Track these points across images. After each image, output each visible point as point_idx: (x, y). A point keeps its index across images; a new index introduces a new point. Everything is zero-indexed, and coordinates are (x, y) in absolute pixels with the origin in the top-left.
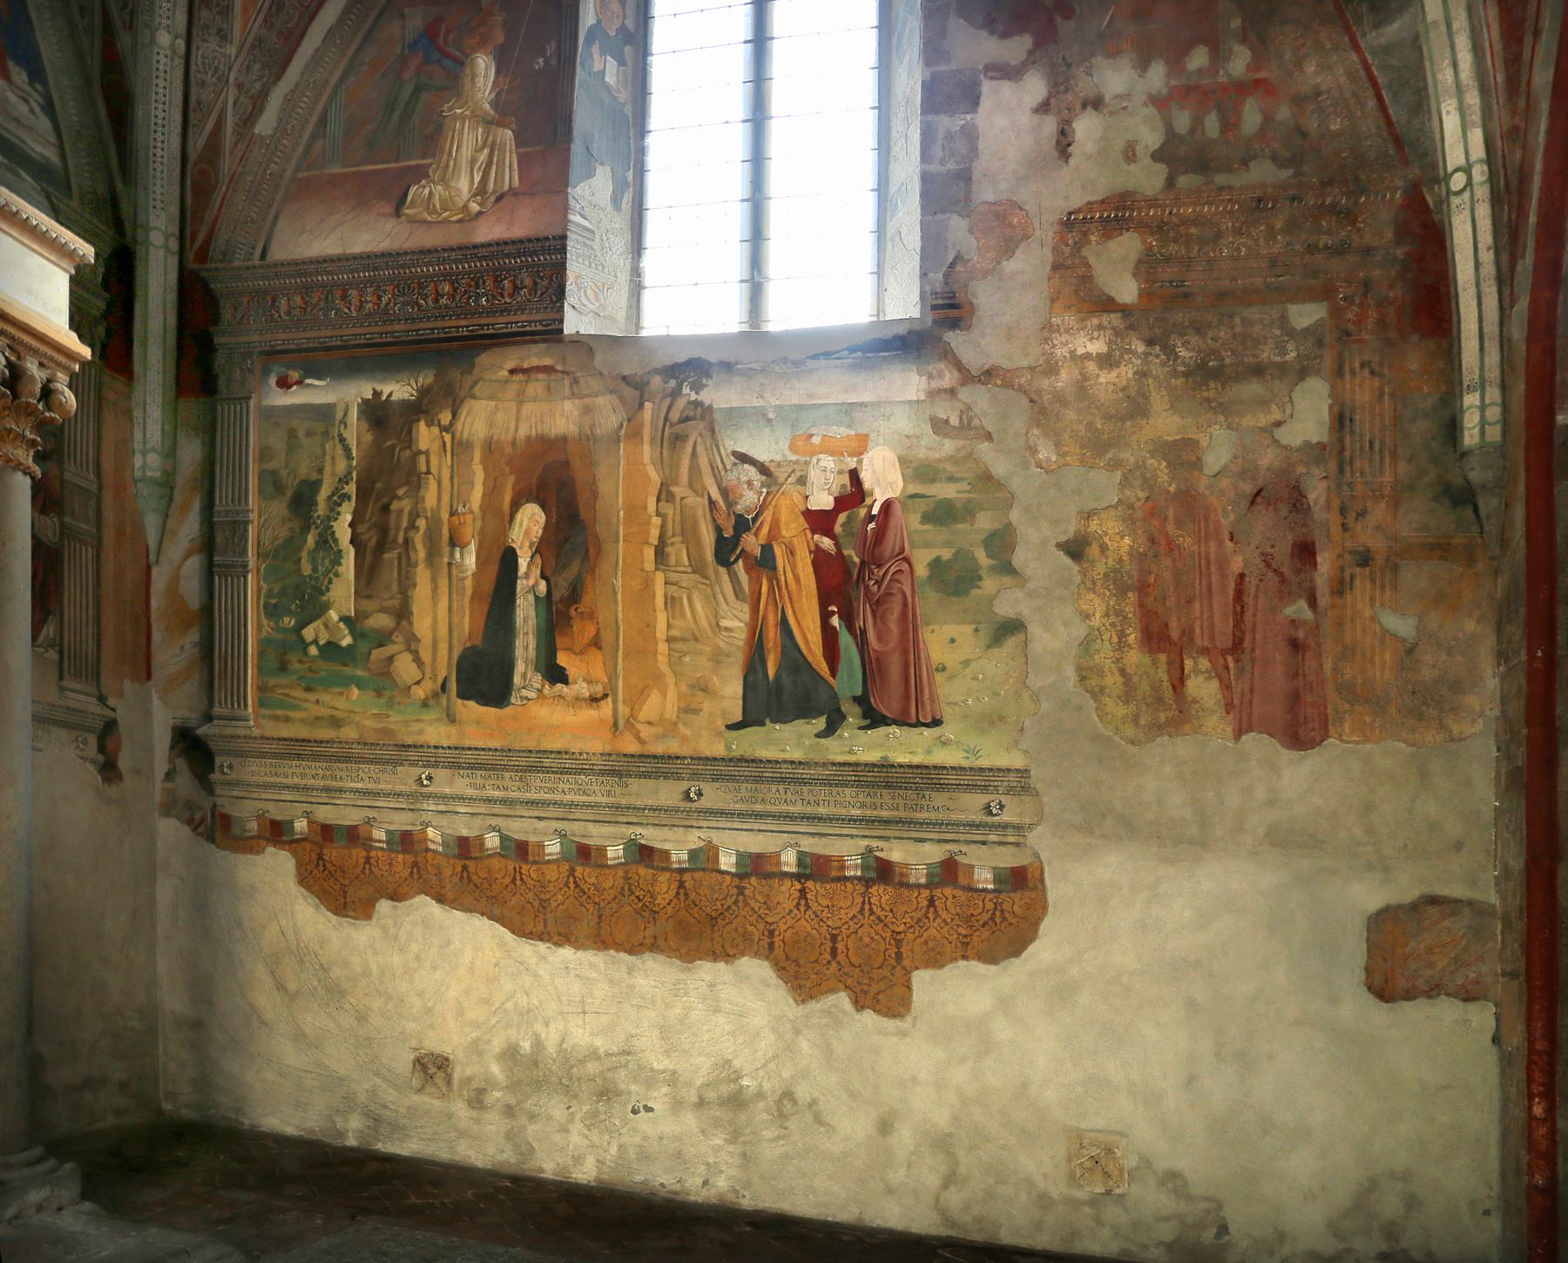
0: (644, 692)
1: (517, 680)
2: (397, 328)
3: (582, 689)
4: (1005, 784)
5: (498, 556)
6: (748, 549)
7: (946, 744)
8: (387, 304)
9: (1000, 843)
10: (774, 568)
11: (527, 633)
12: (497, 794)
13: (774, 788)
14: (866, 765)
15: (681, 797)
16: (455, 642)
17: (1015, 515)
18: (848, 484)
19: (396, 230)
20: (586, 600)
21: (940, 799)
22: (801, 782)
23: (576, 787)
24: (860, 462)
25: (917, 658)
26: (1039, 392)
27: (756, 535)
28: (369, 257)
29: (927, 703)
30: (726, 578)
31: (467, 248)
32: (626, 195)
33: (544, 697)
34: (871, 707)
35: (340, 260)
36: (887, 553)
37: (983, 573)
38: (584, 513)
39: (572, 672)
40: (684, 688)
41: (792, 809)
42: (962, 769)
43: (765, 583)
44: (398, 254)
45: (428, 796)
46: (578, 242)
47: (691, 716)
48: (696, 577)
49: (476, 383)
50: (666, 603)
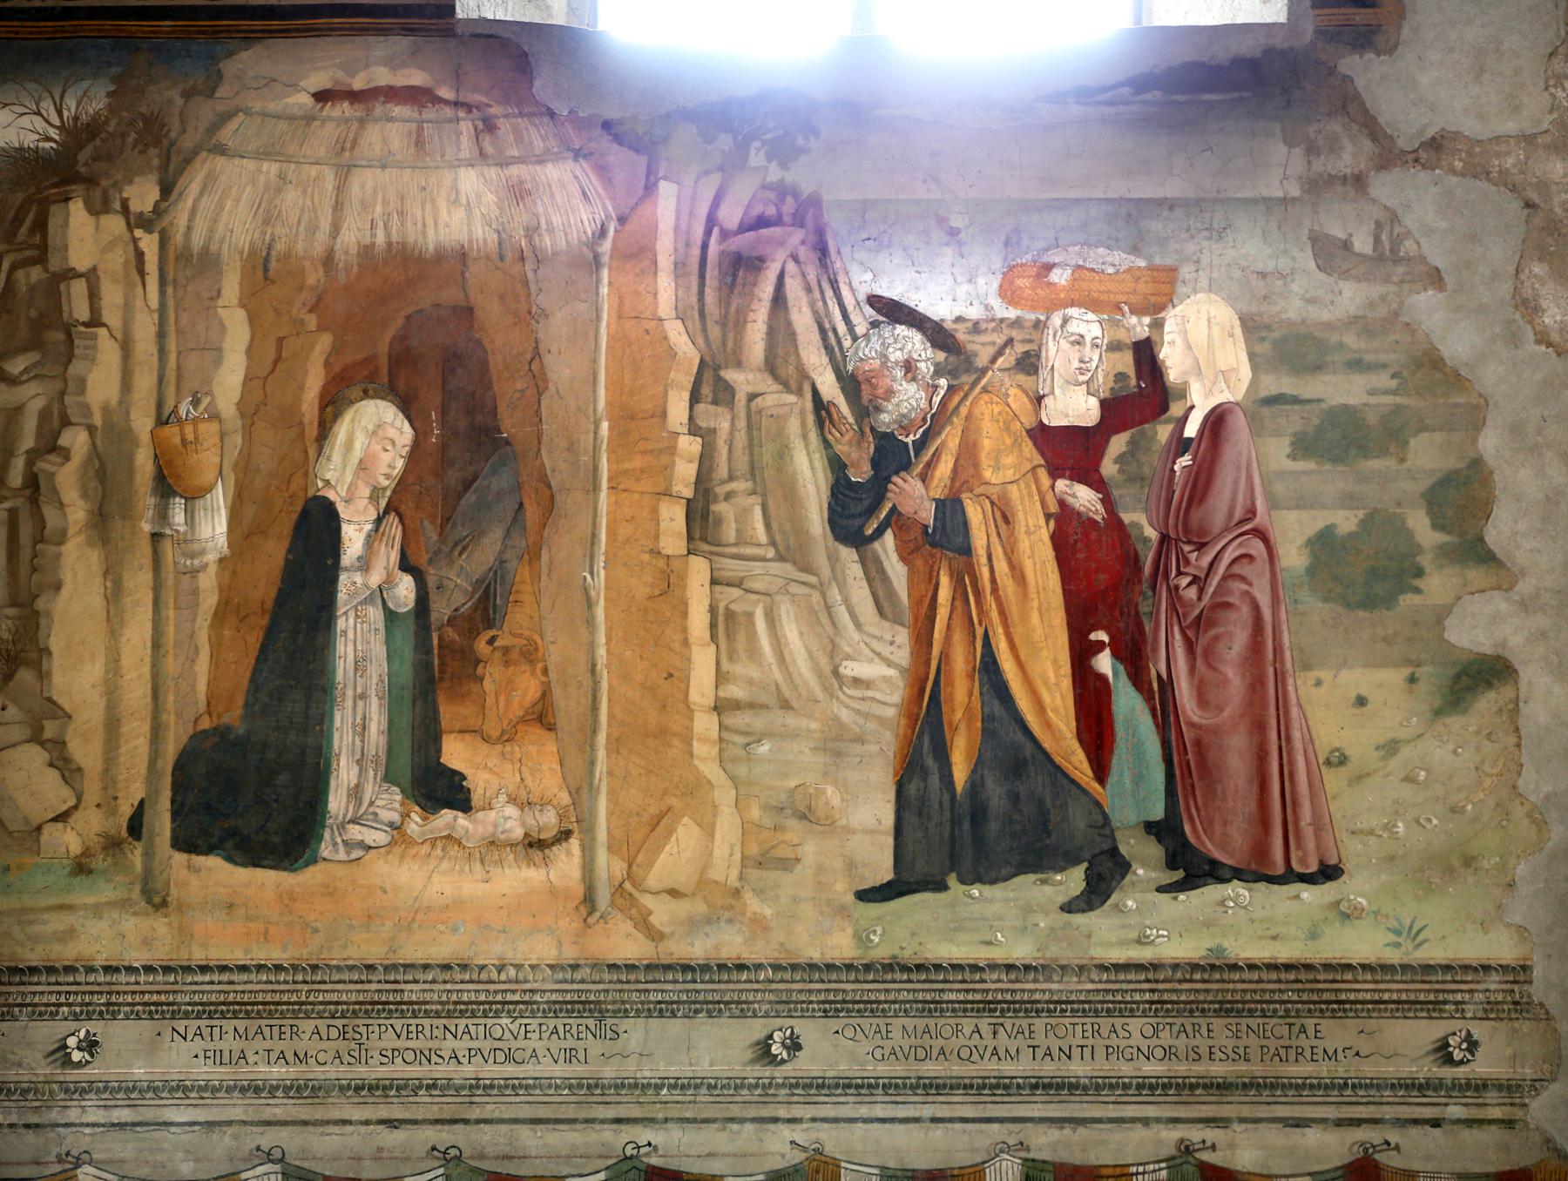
0: (658, 824)
1: (336, 803)
3: (509, 821)
4: (1479, 997)
5: (286, 525)
6: (906, 508)
7: (1346, 914)
9: (1471, 1123)
10: (967, 551)
11: (363, 696)
12: (278, 1072)
13: (968, 1025)
14: (1176, 967)
15: (749, 1055)
16: (170, 718)
17: (1489, 443)
18: (1132, 372)
20: (518, 621)
21: (1337, 1033)
22: (1031, 1008)
23: (487, 1045)
24: (1158, 325)
25: (1285, 737)
26: (1543, 186)
27: (924, 478)
29: (1308, 832)
30: (855, 570)
33: (409, 842)
34: (1185, 843)
36: (1218, 520)
37: (1425, 560)
38: (510, 424)
39: (479, 783)
40: (755, 813)
41: (1008, 1068)
42: (1386, 968)
43: (945, 581)
45: (82, 1090)
47: (772, 875)
48: (788, 569)
50: (713, 626)
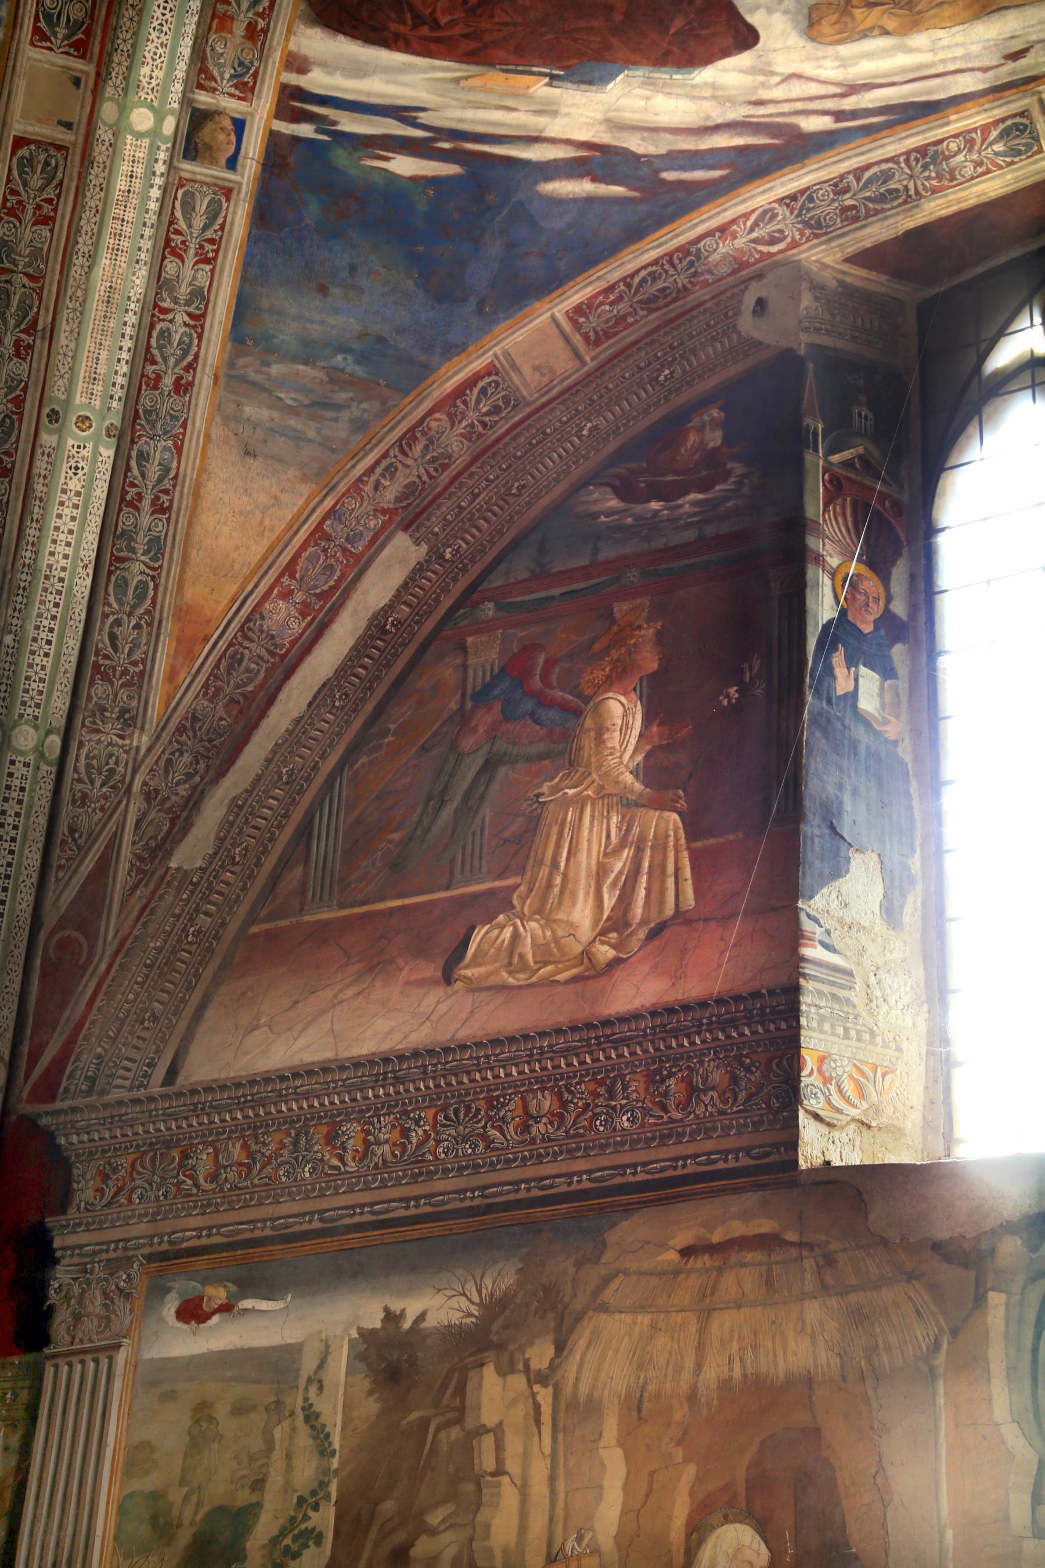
2: (441, 1186)
8: (421, 1144)
19: (443, 1008)
28: (386, 1060)
31: (589, 1026)
32: (910, 898)
35: (326, 1070)
44: (447, 1050)
46: (820, 993)
49: (607, 1280)
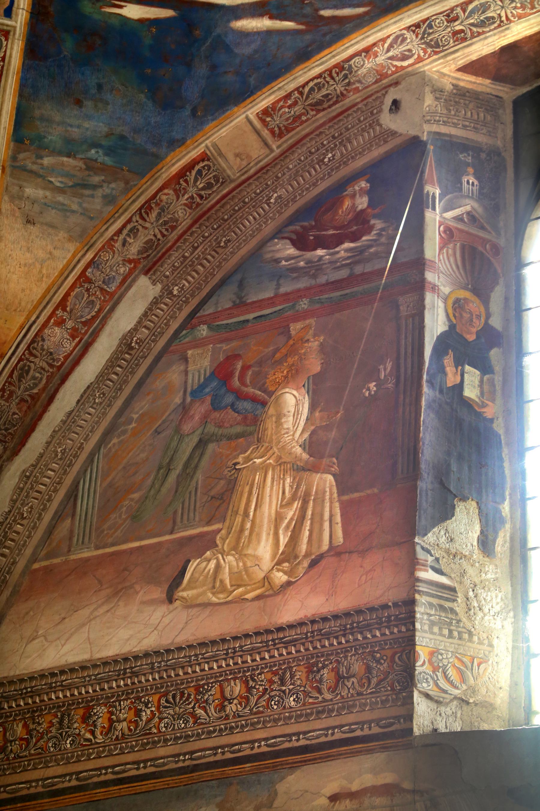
2: (162, 751)
8: (149, 721)
31: (268, 632)
44: (168, 651)
